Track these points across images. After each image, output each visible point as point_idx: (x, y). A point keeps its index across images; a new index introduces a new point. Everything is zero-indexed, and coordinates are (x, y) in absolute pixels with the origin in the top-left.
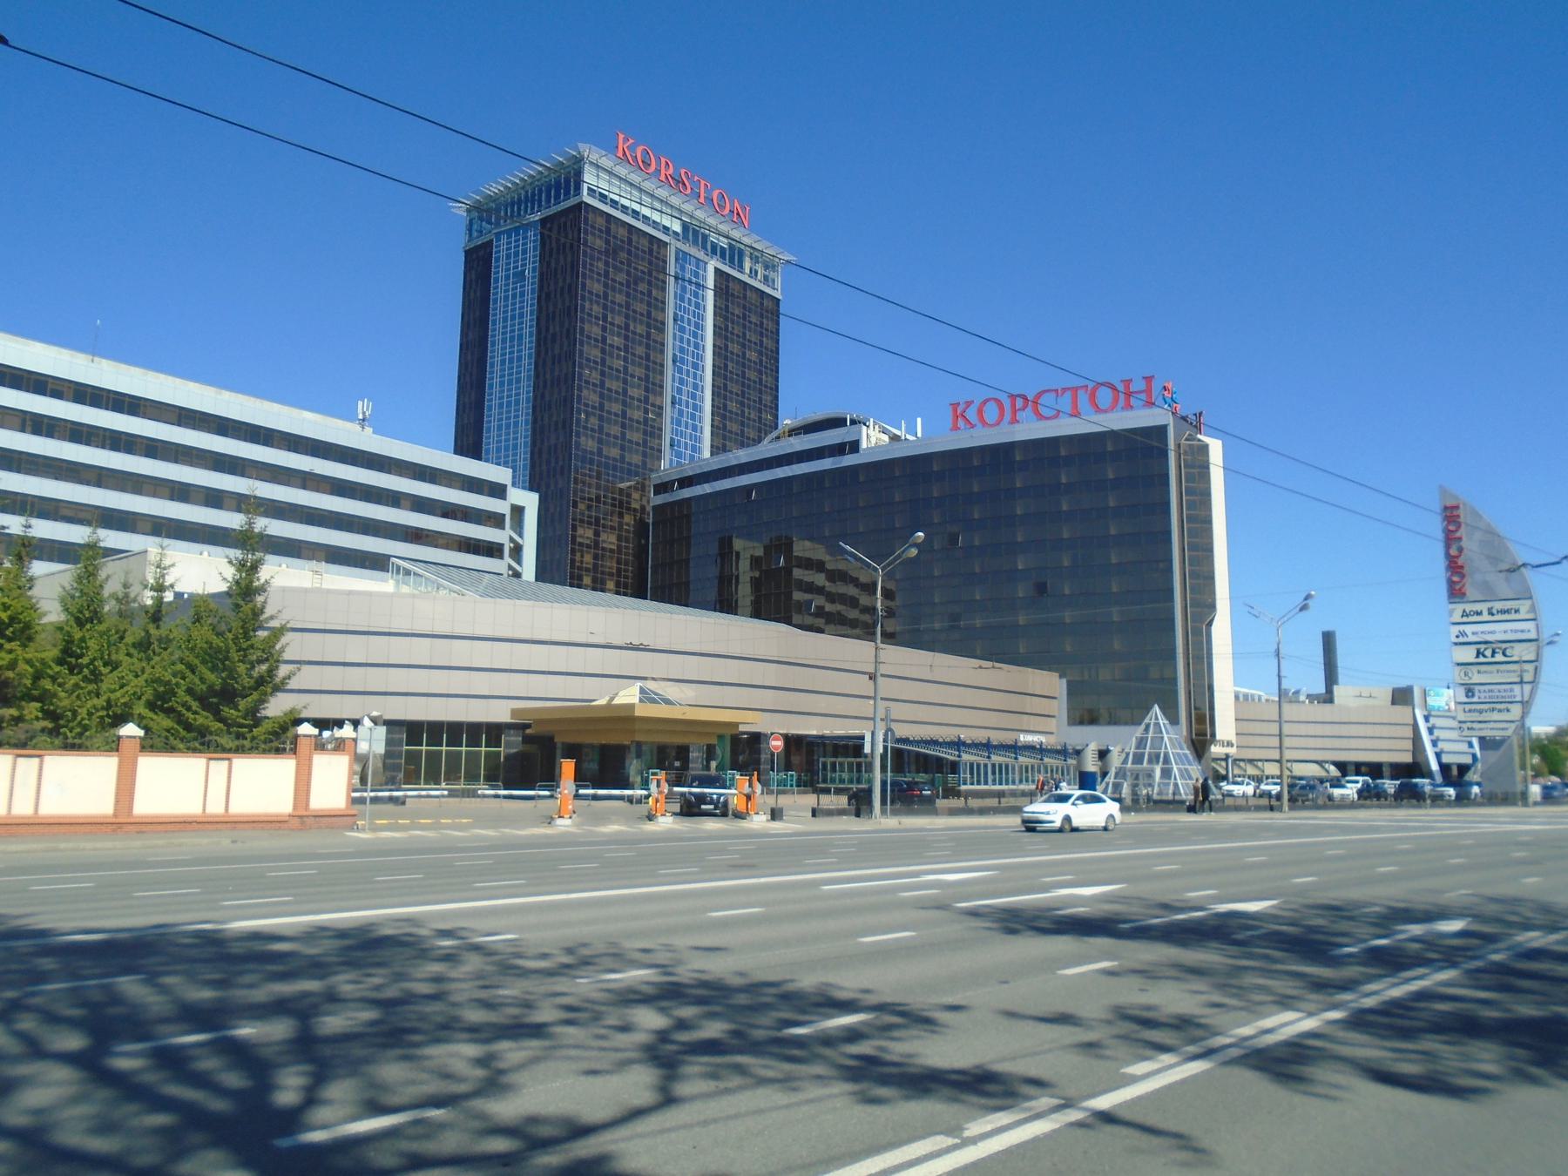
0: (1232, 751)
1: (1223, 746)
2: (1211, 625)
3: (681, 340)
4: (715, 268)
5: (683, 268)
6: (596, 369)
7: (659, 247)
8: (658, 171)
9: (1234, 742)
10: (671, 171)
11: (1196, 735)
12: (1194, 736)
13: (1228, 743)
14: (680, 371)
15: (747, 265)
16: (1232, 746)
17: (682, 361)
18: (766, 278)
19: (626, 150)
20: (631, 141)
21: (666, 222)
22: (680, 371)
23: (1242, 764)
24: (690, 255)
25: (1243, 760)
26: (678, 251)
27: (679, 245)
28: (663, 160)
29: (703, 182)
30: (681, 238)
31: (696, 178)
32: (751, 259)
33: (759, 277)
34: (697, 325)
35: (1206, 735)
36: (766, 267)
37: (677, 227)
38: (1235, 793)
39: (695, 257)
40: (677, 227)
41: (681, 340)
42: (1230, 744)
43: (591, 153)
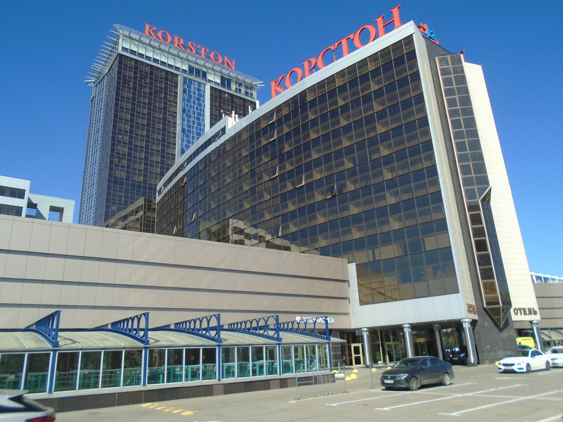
0: (536, 318)
1: (525, 314)
2: (489, 201)
3: (189, 121)
4: (211, 86)
5: (189, 87)
6: (127, 135)
7: (172, 77)
8: (172, 42)
9: (536, 309)
10: (182, 42)
11: (488, 304)
12: (485, 306)
13: (530, 310)
14: (188, 136)
15: (233, 86)
16: (535, 313)
17: (189, 131)
18: (247, 93)
19: (150, 31)
20: (154, 28)
21: (178, 65)
22: (188, 136)
23: (546, 332)
24: (194, 80)
25: (546, 329)
26: (185, 79)
27: (185, 75)
28: (176, 38)
29: (203, 49)
30: (188, 73)
31: (199, 47)
32: (237, 83)
33: (242, 92)
34: (199, 114)
35: (498, 303)
36: (247, 87)
37: (186, 68)
38: (515, 368)
39: (197, 82)
40: (186, 68)
41: (189, 121)
42: (531, 312)
43: (123, 31)
